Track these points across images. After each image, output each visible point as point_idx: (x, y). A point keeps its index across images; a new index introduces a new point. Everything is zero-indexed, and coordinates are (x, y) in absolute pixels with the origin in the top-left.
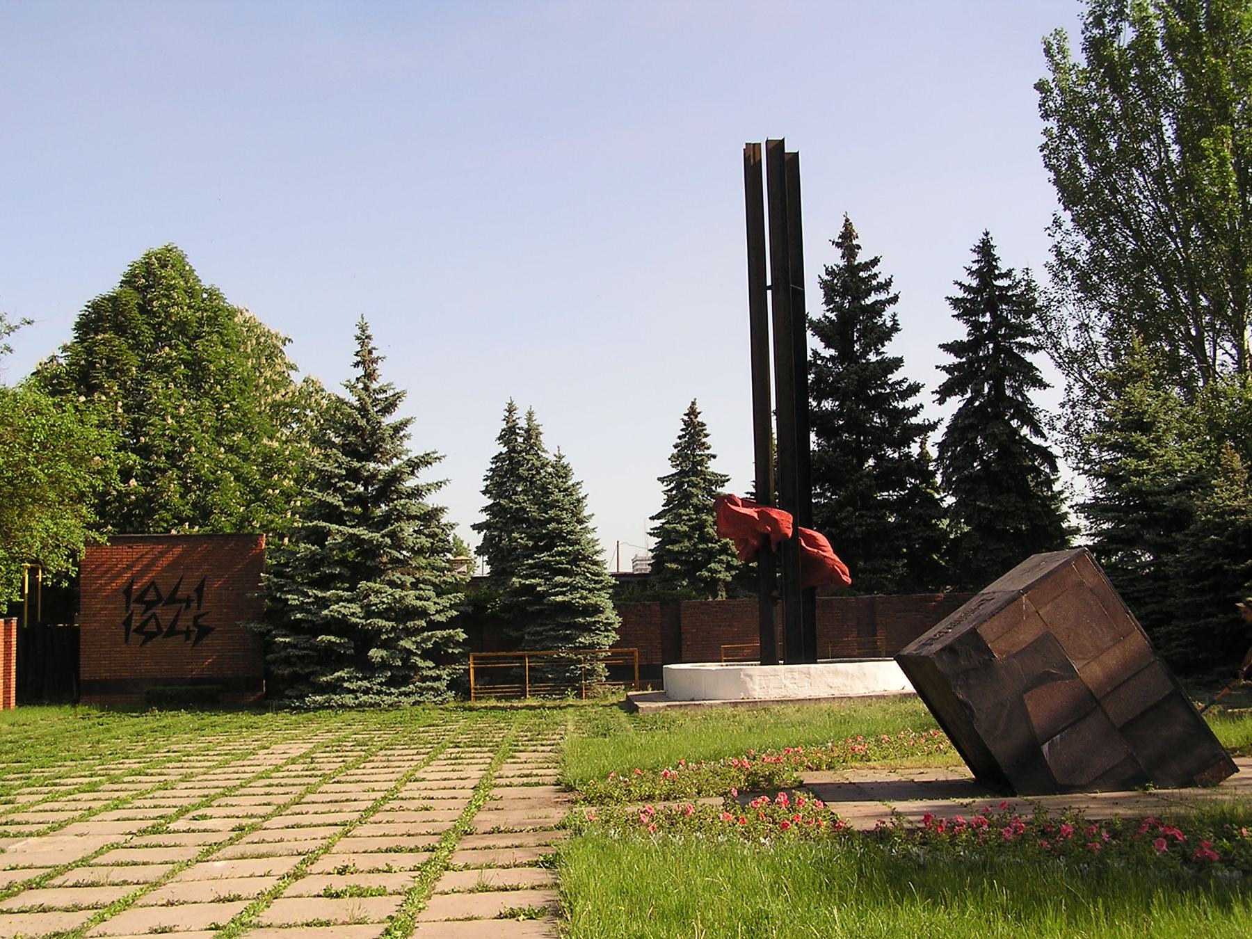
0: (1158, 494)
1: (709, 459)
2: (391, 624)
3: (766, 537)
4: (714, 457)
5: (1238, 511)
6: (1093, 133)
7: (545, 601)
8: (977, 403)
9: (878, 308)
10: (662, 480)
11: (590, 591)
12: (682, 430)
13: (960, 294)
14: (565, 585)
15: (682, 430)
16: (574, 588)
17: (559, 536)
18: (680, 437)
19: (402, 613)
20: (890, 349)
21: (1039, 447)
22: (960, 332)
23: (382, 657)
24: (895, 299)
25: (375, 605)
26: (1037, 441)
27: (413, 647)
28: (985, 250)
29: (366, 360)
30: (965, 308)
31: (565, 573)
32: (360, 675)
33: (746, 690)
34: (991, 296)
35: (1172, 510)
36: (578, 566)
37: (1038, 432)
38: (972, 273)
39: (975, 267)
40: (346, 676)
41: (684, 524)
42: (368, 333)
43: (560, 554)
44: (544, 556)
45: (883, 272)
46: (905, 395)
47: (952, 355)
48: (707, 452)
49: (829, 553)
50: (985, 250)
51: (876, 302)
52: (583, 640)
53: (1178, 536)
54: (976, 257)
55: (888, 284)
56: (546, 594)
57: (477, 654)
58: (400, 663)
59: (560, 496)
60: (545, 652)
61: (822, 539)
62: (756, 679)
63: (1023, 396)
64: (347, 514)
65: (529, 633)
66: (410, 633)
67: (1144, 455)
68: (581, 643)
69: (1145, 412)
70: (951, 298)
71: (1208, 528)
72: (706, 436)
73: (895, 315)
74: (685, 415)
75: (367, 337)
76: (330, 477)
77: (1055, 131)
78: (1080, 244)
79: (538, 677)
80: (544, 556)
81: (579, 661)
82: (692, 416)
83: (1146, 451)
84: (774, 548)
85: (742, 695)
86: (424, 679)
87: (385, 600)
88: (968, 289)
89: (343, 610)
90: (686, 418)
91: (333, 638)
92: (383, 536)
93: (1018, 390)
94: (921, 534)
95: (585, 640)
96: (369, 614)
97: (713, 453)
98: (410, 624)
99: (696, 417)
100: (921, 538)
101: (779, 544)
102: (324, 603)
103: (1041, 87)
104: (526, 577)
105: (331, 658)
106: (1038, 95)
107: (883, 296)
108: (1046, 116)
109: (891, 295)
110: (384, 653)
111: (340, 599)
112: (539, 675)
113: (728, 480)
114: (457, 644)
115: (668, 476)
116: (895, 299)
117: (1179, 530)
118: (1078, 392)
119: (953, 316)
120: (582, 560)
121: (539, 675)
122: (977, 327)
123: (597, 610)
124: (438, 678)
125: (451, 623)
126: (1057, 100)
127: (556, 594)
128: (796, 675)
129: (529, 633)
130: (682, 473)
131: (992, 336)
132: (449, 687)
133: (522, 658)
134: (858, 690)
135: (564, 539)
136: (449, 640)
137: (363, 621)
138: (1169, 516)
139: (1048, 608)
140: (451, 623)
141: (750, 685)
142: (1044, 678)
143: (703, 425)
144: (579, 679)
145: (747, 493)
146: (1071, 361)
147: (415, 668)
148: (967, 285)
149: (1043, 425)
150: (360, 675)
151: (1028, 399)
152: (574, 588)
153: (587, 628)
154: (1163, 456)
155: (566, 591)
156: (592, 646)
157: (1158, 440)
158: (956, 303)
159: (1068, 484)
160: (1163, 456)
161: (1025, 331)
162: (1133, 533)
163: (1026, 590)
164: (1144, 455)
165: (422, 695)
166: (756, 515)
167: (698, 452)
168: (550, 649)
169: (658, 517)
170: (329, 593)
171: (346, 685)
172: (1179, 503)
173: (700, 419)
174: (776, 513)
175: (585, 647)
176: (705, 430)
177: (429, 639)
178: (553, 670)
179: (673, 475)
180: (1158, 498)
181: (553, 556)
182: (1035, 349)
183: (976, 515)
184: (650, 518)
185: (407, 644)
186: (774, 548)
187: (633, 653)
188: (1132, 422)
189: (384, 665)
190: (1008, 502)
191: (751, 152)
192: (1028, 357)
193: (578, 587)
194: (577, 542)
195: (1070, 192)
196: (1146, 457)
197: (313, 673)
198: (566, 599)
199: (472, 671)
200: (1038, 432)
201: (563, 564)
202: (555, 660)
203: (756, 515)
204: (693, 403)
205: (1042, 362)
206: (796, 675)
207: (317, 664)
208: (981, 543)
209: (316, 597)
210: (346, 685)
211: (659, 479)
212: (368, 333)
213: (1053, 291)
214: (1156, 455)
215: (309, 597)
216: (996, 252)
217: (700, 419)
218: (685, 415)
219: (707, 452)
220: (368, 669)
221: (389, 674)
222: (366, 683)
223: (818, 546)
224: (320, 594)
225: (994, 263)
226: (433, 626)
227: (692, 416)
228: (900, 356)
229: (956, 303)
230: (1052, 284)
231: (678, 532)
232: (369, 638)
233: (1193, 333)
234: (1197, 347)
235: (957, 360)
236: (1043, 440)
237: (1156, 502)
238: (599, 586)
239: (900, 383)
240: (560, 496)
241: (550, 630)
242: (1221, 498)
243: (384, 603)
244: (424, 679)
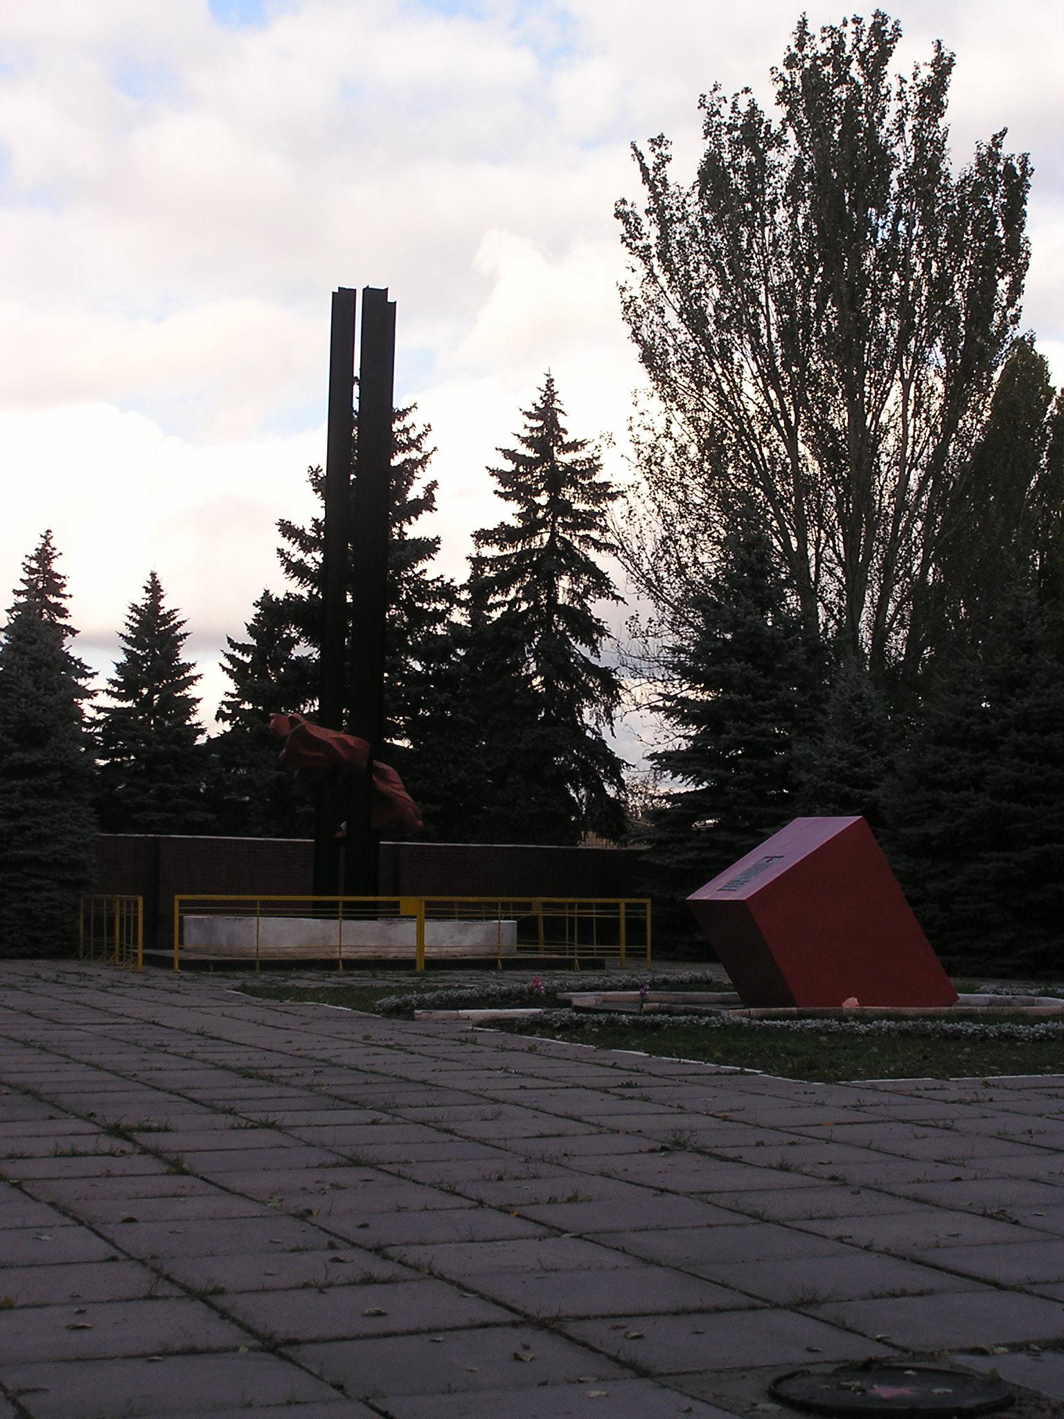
9: (406, 473)
13: (509, 466)
22: (509, 513)
28: (547, 413)
38: (524, 440)
50: (547, 413)
119: (496, 492)
158: (503, 477)
191: (342, 300)
216: (562, 421)
228: (431, 536)
229: (503, 477)
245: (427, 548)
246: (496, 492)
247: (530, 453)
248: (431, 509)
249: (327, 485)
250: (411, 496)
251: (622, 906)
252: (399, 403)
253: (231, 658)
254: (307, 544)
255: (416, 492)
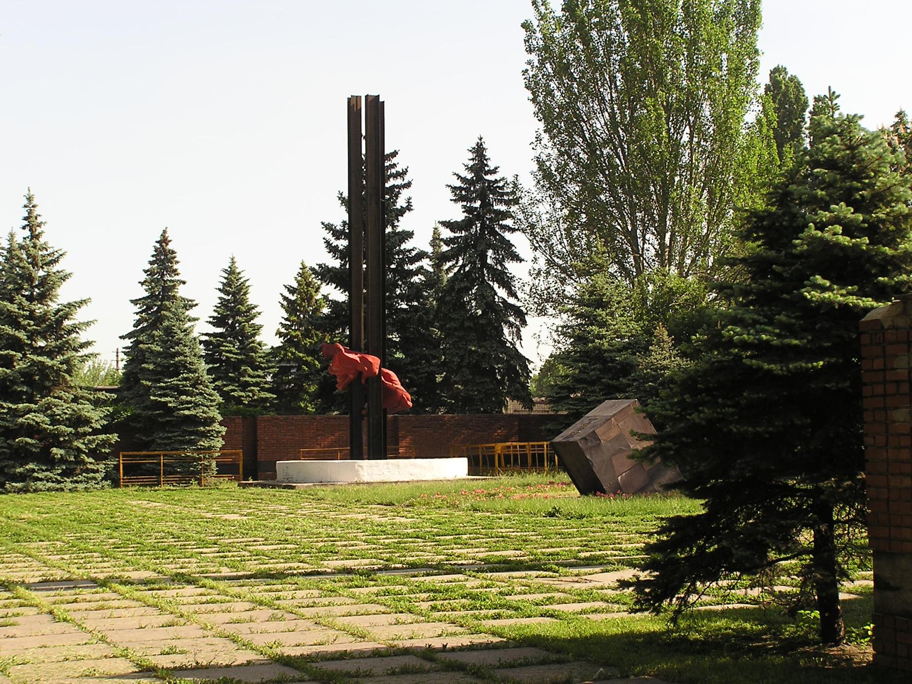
0: (611, 351)
1: (179, 284)
2: (70, 429)
3: (360, 374)
4: (184, 283)
5: (665, 368)
6: (562, 70)
7: (175, 414)
8: (467, 269)
9: (394, 192)
10: (135, 302)
11: (207, 406)
12: (153, 256)
13: (458, 184)
14: (190, 402)
15: (153, 256)
16: (197, 405)
17: (184, 366)
18: (151, 263)
19: (78, 421)
20: (404, 224)
21: (513, 306)
22: (457, 213)
23: (61, 455)
24: (408, 185)
25: (59, 415)
26: (512, 301)
27: (83, 447)
28: (479, 151)
29: (31, 223)
30: (460, 194)
31: (187, 393)
32: (44, 468)
33: (358, 476)
34: (483, 188)
35: (621, 363)
36: (197, 389)
37: (512, 294)
39: (471, 163)
40: (36, 468)
41: (157, 344)
42: (34, 203)
43: (186, 379)
44: (174, 381)
45: (400, 163)
46: (413, 260)
47: (448, 230)
48: (176, 278)
49: (399, 386)
50: (479, 151)
51: (394, 186)
52: (202, 443)
53: (624, 381)
54: (471, 156)
55: (404, 173)
56: (176, 409)
57: (126, 453)
58: (72, 459)
59: (181, 335)
60: (175, 452)
61: (394, 376)
62: (365, 468)
63: (502, 265)
64: (27, 345)
65: (160, 438)
66: (78, 436)
67: (603, 324)
68: (201, 445)
69: (604, 295)
70: (450, 186)
71: (646, 378)
72: (177, 262)
73: (410, 199)
74: (157, 242)
75: (34, 206)
76: (17, 317)
77: (536, 64)
78: (550, 151)
79: (170, 471)
80: (174, 381)
81: (200, 459)
82: (164, 244)
83: (605, 322)
84: (363, 382)
85: (356, 479)
86: (88, 471)
87: (66, 411)
88: (463, 180)
89: (36, 419)
90: (158, 245)
91: (28, 440)
92: (61, 363)
93: (500, 262)
94: (427, 369)
95: (204, 443)
96: (54, 422)
97: (183, 279)
98: (81, 430)
99: (167, 244)
100: (427, 372)
101: (367, 380)
102: (15, 413)
103: (526, 26)
104: (160, 396)
105: (23, 454)
106: (523, 33)
107: (399, 182)
108: (530, 51)
109: (406, 181)
110: (62, 452)
111: (30, 411)
112: (169, 469)
113: (196, 305)
114: (111, 445)
115: (140, 299)
116: (408, 185)
117: (624, 377)
118: (542, 264)
119: (451, 200)
120: (200, 384)
121: (169, 469)
122: (468, 210)
123: (212, 420)
124: (97, 471)
125: (105, 430)
126: (538, 40)
127: (183, 409)
128: (390, 466)
129: (160, 438)
130: (152, 296)
131: (479, 217)
132: (105, 478)
133: (160, 456)
134: (429, 476)
135: (186, 368)
136: (104, 443)
137: (51, 427)
138: (618, 367)
139: (622, 423)
140: (105, 430)
141: (361, 473)
142: (621, 451)
143: (173, 252)
144: (199, 473)
145: (210, 317)
146: (540, 241)
147: (83, 462)
148: (463, 176)
149: (517, 289)
150: (44, 468)
151: (506, 268)
152: (197, 405)
153: (204, 435)
154: (614, 325)
155: (191, 407)
156: (210, 448)
157: (612, 314)
158: (454, 189)
159: (537, 335)
160: (614, 325)
161: (506, 215)
162: (595, 378)
163: (613, 416)
164: (603, 324)
165: (88, 483)
166: (358, 359)
167: (167, 278)
168: (177, 450)
169: (130, 336)
170: (21, 406)
171: (36, 474)
172: (626, 358)
173: (170, 247)
174: (371, 358)
175: (205, 449)
176: (175, 257)
177: (94, 440)
178: (180, 465)
179: (144, 298)
180: (612, 355)
181: (179, 381)
182: (513, 230)
183: (467, 356)
184: (121, 337)
185: (78, 444)
186: (363, 382)
187: (238, 454)
188: (596, 300)
189: (62, 460)
190: (492, 347)
192: (507, 236)
193: (199, 405)
194: (195, 371)
195: (546, 114)
196: (604, 326)
197: (6, 466)
198: (191, 413)
199: (121, 466)
200: (512, 294)
201: (187, 386)
202: (181, 458)
203: (358, 359)
204: (165, 232)
205: (520, 242)
206: (390, 466)
207: (9, 459)
208: (471, 377)
209: (10, 409)
210: (36, 474)
211: (132, 301)
212: (34, 203)
213: (536, 193)
214: (610, 325)
215: (4, 408)
216: (488, 154)
217: (170, 247)
218: (157, 242)
219: (176, 278)
220: (50, 462)
221: (64, 468)
222: (48, 473)
223: (392, 381)
224: (14, 407)
225: (485, 162)
226: (96, 432)
227: (164, 244)
229: (454, 189)
230: (535, 189)
231: (152, 352)
232: (54, 439)
233: (630, 228)
234: (632, 237)
235: (452, 235)
236: (516, 300)
237: (611, 357)
238: (214, 404)
239: (410, 251)
240: (181, 335)
241: (178, 436)
242: (656, 359)
243: (66, 413)
244: (88, 471)
245: (409, 235)
246: (451, 200)
247: (469, 176)
248: (410, 210)
249: (349, 203)
250: (398, 206)
251: (527, 447)
252: (387, 151)
253: (285, 298)
254: (337, 234)
255: (401, 203)
